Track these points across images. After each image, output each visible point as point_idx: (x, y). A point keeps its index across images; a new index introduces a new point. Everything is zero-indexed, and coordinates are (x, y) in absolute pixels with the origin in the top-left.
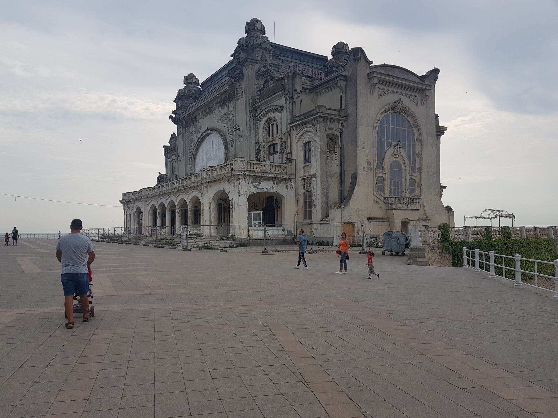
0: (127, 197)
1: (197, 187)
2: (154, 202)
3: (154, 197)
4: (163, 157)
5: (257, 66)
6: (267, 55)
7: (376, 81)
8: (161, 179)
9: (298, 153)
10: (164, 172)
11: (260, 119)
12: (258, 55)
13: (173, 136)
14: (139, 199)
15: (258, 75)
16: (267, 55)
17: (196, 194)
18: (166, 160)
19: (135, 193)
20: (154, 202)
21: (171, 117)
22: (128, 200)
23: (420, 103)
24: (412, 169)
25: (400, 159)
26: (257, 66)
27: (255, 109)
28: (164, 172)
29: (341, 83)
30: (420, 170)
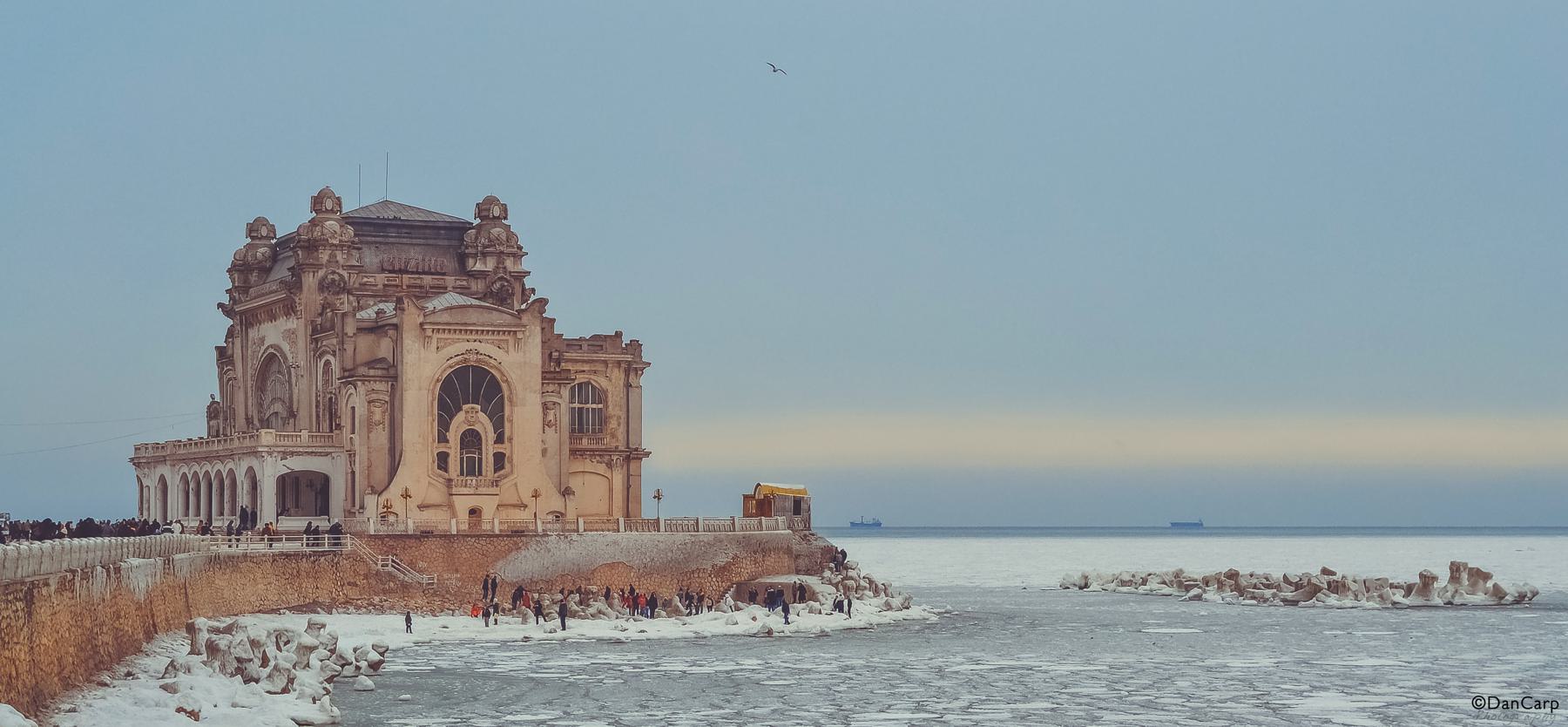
0: (142, 453)
1: (231, 456)
2: (185, 469)
3: (185, 460)
4: (216, 370)
5: (321, 273)
6: (339, 254)
7: (429, 333)
8: (213, 412)
9: (345, 421)
10: (218, 399)
11: (320, 356)
12: (324, 256)
13: (230, 334)
14: (162, 460)
15: (323, 286)
16: (339, 254)
17: (231, 465)
18: (221, 379)
19: (156, 446)
20: (185, 469)
21: (220, 305)
22: (146, 458)
23: (511, 349)
24: (500, 439)
25: (477, 427)
26: (321, 273)
27: (316, 340)
28: (218, 399)
29: (391, 332)
30: (510, 439)
